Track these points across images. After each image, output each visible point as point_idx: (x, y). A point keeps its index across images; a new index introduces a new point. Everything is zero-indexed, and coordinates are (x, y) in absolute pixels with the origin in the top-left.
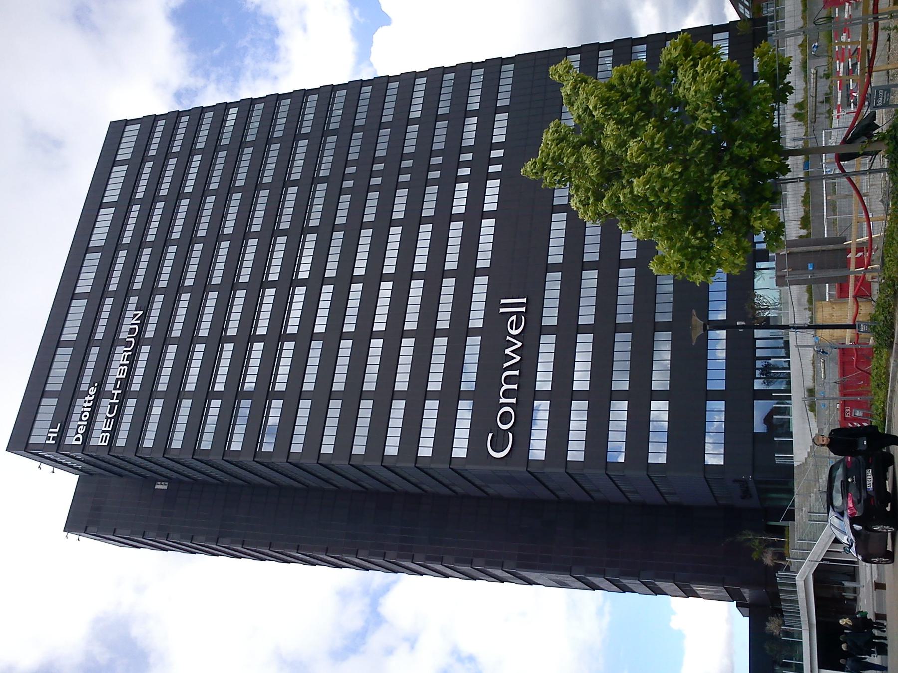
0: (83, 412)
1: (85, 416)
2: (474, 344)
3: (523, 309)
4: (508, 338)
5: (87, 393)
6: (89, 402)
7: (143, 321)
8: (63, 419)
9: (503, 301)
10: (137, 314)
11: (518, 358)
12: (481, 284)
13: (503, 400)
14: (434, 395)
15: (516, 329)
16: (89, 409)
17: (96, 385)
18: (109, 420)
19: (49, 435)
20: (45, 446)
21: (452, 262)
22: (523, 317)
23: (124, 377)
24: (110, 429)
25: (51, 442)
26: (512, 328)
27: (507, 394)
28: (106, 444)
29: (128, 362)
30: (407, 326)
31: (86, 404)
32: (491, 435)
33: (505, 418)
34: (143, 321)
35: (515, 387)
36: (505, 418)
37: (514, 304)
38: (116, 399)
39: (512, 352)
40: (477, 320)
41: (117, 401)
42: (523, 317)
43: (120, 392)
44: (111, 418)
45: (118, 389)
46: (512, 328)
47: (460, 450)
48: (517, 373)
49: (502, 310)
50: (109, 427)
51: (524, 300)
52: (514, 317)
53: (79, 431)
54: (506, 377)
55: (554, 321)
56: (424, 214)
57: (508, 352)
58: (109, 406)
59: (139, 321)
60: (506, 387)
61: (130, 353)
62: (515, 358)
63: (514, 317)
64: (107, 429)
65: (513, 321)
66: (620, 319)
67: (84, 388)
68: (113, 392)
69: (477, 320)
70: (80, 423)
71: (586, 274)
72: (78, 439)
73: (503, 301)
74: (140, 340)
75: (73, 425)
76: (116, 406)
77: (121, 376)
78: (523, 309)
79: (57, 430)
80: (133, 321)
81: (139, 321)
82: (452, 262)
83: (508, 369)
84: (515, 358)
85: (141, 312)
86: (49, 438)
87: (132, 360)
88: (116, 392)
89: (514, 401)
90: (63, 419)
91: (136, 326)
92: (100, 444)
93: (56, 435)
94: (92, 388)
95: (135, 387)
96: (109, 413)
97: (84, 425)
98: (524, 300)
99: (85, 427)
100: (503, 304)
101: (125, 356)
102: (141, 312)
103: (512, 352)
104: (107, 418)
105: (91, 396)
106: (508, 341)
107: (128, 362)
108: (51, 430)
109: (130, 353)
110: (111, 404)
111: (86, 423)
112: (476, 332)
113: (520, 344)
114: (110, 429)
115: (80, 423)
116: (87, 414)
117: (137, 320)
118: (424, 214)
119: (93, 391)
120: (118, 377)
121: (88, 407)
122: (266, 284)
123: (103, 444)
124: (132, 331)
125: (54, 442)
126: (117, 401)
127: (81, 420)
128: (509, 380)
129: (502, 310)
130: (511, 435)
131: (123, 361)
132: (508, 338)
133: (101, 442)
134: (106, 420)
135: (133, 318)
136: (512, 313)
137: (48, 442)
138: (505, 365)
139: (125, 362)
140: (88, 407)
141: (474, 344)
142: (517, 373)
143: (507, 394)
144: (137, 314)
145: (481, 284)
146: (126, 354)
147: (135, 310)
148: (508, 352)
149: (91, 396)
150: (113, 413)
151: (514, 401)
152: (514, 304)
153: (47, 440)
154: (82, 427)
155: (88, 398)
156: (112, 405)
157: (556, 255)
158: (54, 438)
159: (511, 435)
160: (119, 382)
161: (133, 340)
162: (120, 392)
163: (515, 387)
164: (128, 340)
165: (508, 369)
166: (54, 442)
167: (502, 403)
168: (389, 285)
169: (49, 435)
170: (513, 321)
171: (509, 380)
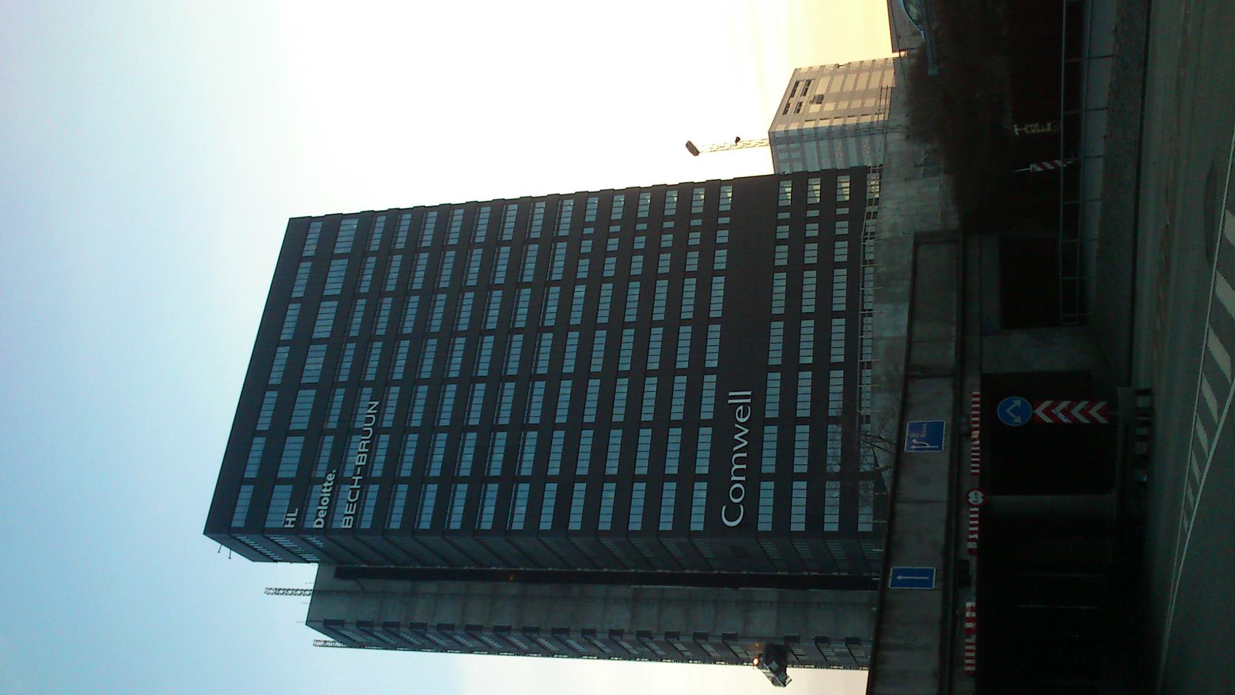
0: (323, 497)
1: (325, 501)
2: (705, 434)
3: (749, 401)
4: (737, 426)
5: (324, 480)
6: (328, 487)
7: (380, 412)
8: (300, 501)
9: (731, 394)
10: (373, 405)
11: (746, 443)
12: (710, 381)
13: (734, 478)
14: (641, 479)
15: (744, 417)
16: (329, 495)
17: (334, 471)
18: (351, 505)
19: (287, 519)
20: (282, 531)
21: (597, 365)
22: (749, 408)
23: (364, 463)
24: (353, 512)
25: (289, 526)
27: (737, 473)
28: (350, 527)
29: (367, 450)
30: (615, 419)
31: (325, 490)
32: (724, 508)
33: (737, 493)
34: (380, 412)
35: (744, 467)
36: (737, 493)
37: (740, 397)
38: (358, 485)
39: (740, 437)
40: (707, 413)
41: (359, 487)
42: (749, 408)
43: (361, 478)
44: (353, 503)
45: (359, 475)
46: (739, 417)
49: (730, 401)
50: (352, 510)
51: (749, 393)
52: (741, 408)
53: (320, 516)
54: (736, 458)
55: (710, 416)
56: (600, 321)
57: (736, 437)
58: (350, 492)
59: (375, 411)
60: (736, 467)
61: (369, 442)
63: (741, 408)
64: (350, 512)
65: (740, 411)
66: (768, 415)
67: (320, 474)
68: (354, 478)
69: (707, 413)
70: (320, 508)
71: (707, 378)
72: (319, 523)
73: (731, 394)
74: (378, 430)
75: (312, 510)
76: (358, 492)
77: (361, 463)
78: (749, 401)
79: (295, 515)
80: (369, 411)
81: (375, 411)
82: (597, 365)
83: (739, 451)
85: (377, 403)
86: (287, 522)
87: (372, 448)
88: (357, 478)
89: (743, 478)
90: (300, 501)
91: (373, 416)
92: (343, 527)
93: (294, 519)
94: (330, 475)
95: (377, 473)
96: (351, 498)
97: (325, 510)
98: (749, 393)
99: (326, 512)
100: (749, 398)
101: (363, 444)
102: (377, 403)
103: (740, 437)
104: (349, 503)
105: (329, 482)
106: (737, 428)
107: (367, 450)
108: (289, 515)
109: (369, 442)
110: (351, 489)
111: (326, 508)
112: (706, 423)
113: (747, 431)
114: (353, 512)
115: (320, 508)
116: (328, 499)
117: (374, 409)
118: (600, 321)
119: (331, 477)
120: (357, 464)
121: (326, 493)
122: (418, 382)
123: (347, 526)
124: (369, 420)
126: (359, 487)
127: (321, 505)
128: (738, 461)
129: (730, 401)
130: (742, 507)
131: (362, 448)
132: (737, 426)
133: (345, 524)
134: (347, 505)
135: (369, 408)
136: (741, 404)
137: (286, 526)
138: (735, 449)
139: (364, 450)
140: (326, 493)
141: (705, 434)
142: (745, 455)
143: (737, 473)
144: (373, 405)
145: (710, 381)
146: (365, 442)
147: (371, 401)
148: (736, 437)
149: (329, 482)
150: (355, 497)
151: (743, 478)
152: (740, 397)
153: (284, 524)
154: (322, 511)
155: (326, 484)
156: (354, 491)
157: (775, 358)
158: (292, 523)
159: (742, 507)
160: (359, 469)
161: (370, 429)
162: (361, 478)
163: (744, 467)
164: (365, 429)
165: (739, 451)
166: (293, 526)
167: (733, 481)
168: (454, 387)
169: (287, 519)
171: (738, 461)
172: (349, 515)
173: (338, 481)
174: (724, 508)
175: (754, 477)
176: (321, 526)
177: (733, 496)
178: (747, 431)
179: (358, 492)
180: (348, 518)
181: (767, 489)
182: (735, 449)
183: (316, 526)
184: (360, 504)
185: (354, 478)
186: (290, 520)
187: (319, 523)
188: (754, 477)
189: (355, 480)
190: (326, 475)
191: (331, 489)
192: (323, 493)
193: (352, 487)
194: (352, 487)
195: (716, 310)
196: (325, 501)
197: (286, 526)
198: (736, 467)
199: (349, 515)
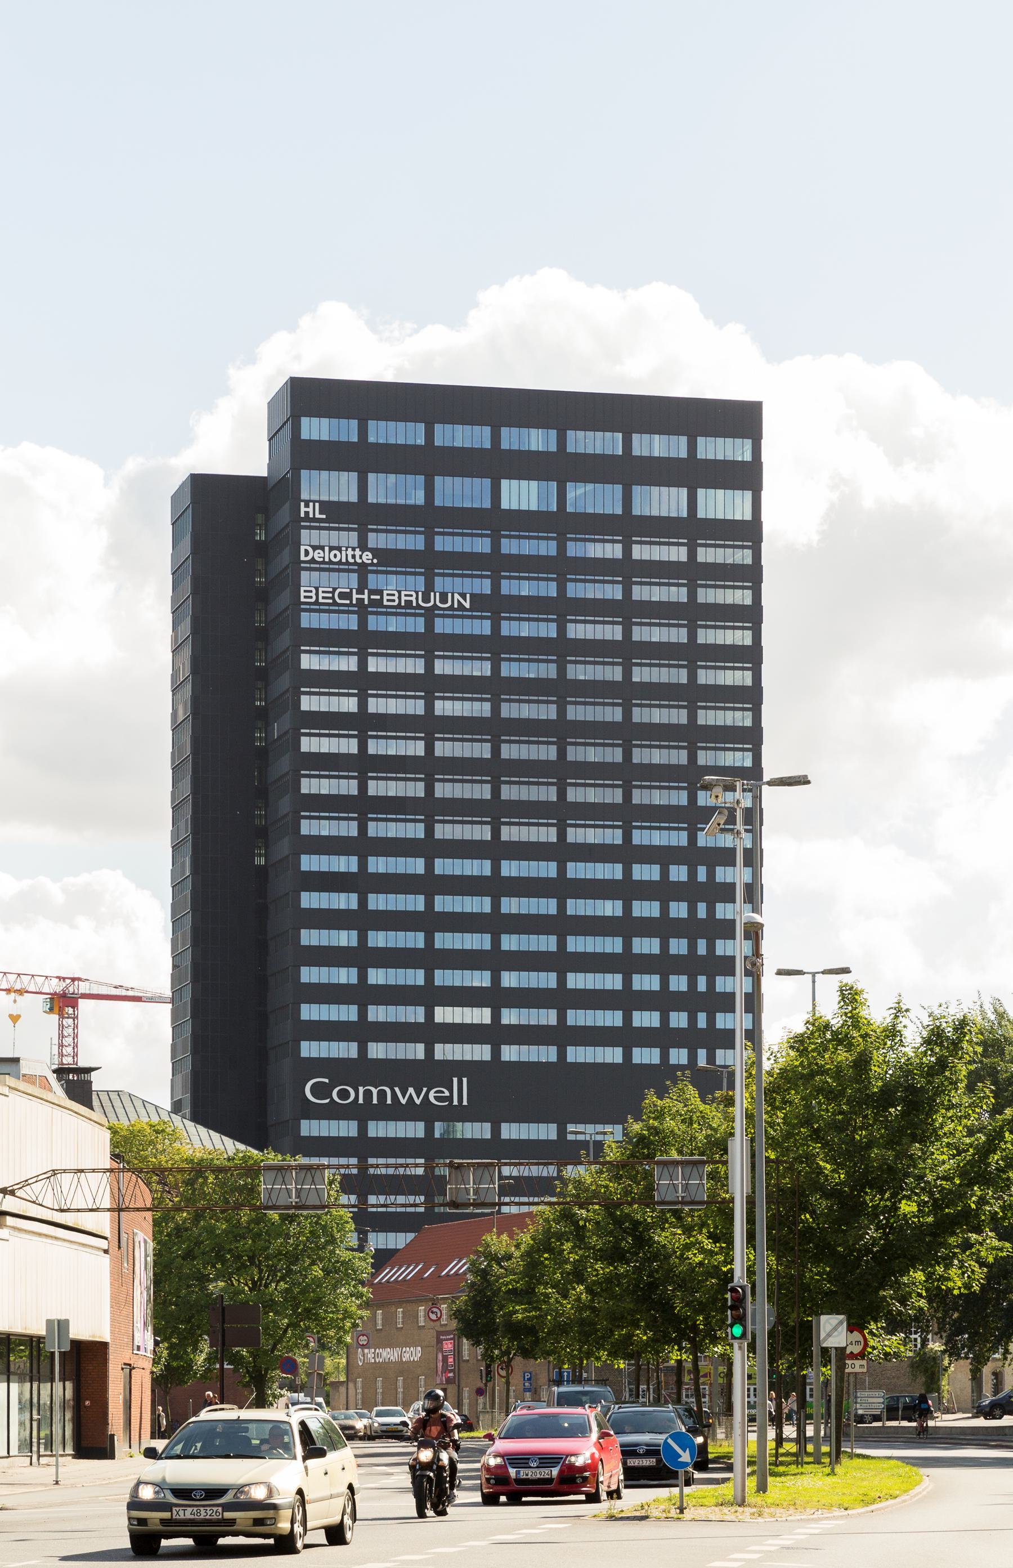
2: (417, 1051)
3: (455, 1103)
4: (425, 1089)
6: (354, 556)
7: (457, 612)
9: (465, 1080)
11: (403, 1101)
12: (481, 1052)
13: (361, 1089)
16: (344, 560)
17: (375, 561)
18: (330, 595)
19: (311, 504)
22: (447, 1103)
24: (321, 600)
25: (303, 509)
26: (435, 1092)
27: (368, 1094)
28: (303, 600)
29: (403, 604)
35: (375, 1101)
37: (460, 1092)
40: (444, 1051)
42: (447, 1103)
44: (333, 598)
46: (436, 1092)
47: (310, 1049)
48: (389, 1101)
49: (455, 1080)
52: (447, 1093)
57: (411, 1090)
60: (375, 1091)
62: (404, 1098)
63: (447, 1093)
64: (321, 595)
65: (443, 1093)
68: (366, 591)
69: (444, 1051)
70: (327, 549)
73: (465, 1080)
74: (430, 615)
77: (385, 597)
78: (455, 1103)
80: (457, 596)
81: (456, 606)
83: (394, 1094)
84: (404, 1098)
85: (467, 605)
87: (407, 609)
88: (365, 597)
89: (361, 1101)
92: (302, 589)
93: (311, 516)
94: (370, 556)
97: (324, 558)
99: (322, 559)
102: (467, 605)
107: (403, 604)
108: (317, 505)
114: (321, 600)
115: (327, 549)
119: (367, 557)
121: (347, 555)
123: (303, 594)
125: (302, 515)
128: (382, 1094)
129: (455, 1080)
132: (425, 1089)
134: (331, 590)
136: (451, 1092)
137: (302, 504)
138: (397, 1089)
139: (403, 598)
140: (347, 555)
141: (417, 1051)
142: (389, 1101)
143: (368, 1094)
145: (481, 1052)
146: (413, 599)
147: (472, 595)
148: (411, 1090)
151: (361, 1101)
155: (358, 552)
156: (347, 596)
162: (366, 602)
163: (375, 1101)
165: (394, 1094)
170: (443, 1093)
171: (382, 1094)
172: (317, 594)
173: (362, 570)
174: (327, 1081)
175: (362, 1113)
176: (303, 558)
177: (340, 1090)
178: (418, 1102)
179: (348, 602)
180: (313, 594)
181: (347, 1129)
182: (397, 1089)
183: (303, 548)
184: (332, 608)
185: (366, 591)
186: (310, 510)
187: (307, 553)
188: (362, 1113)
189: (363, 594)
190: (371, 550)
191: (352, 561)
192: (347, 550)
193: (354, 591)
194: (354, 591)
195: (577, 1054)
196: (335, 556)
197: (302, 504)
198: (375, 1091)
199: (317, 594)
